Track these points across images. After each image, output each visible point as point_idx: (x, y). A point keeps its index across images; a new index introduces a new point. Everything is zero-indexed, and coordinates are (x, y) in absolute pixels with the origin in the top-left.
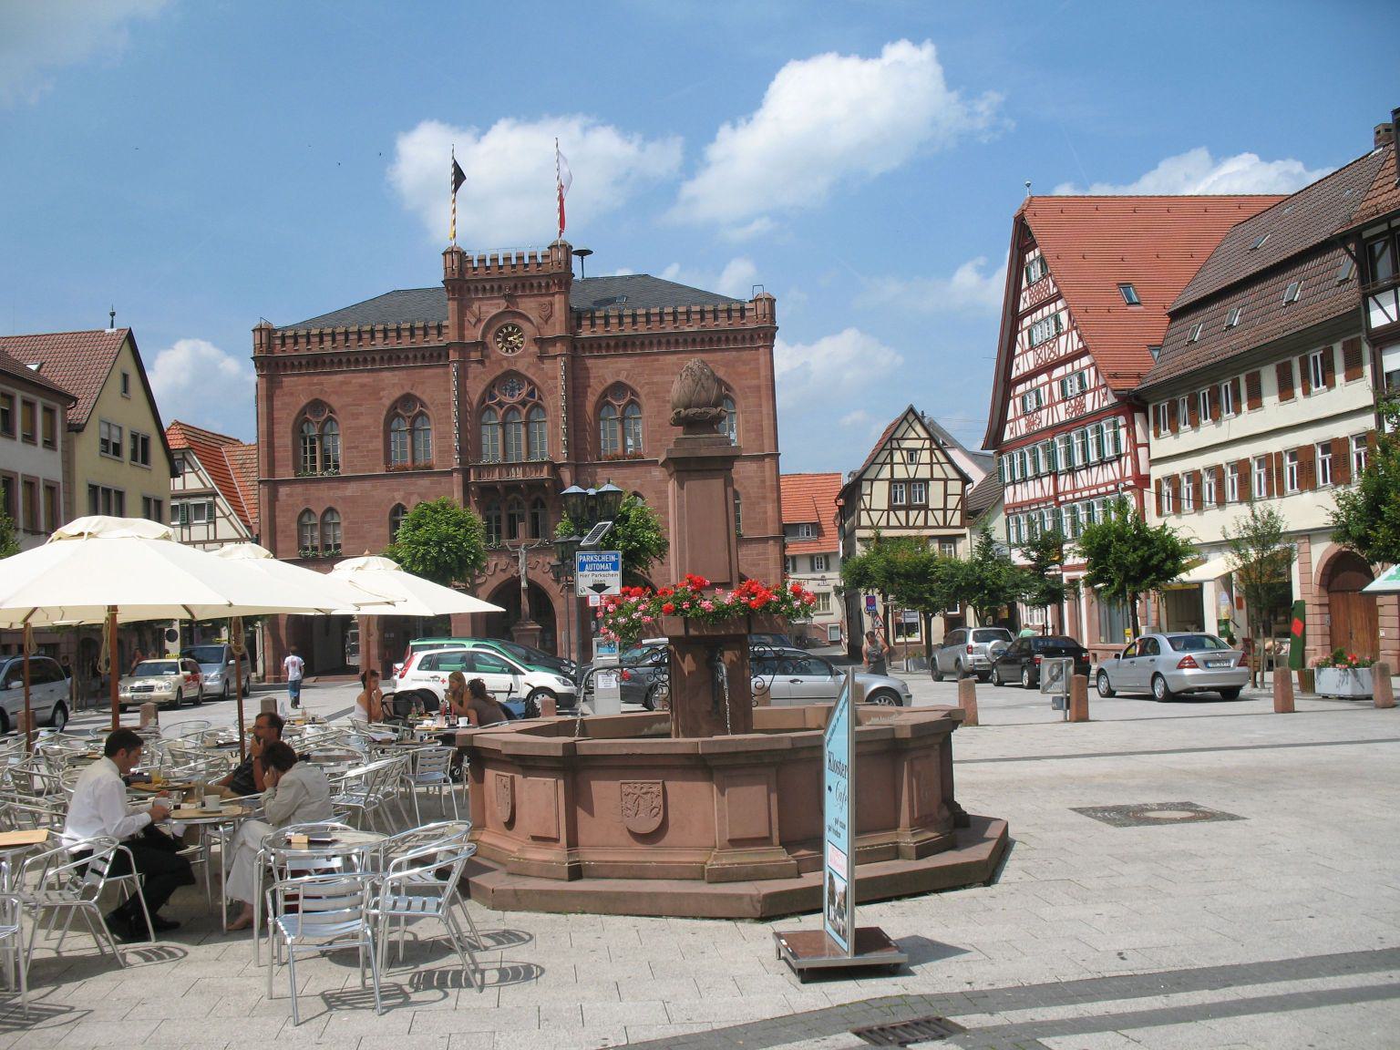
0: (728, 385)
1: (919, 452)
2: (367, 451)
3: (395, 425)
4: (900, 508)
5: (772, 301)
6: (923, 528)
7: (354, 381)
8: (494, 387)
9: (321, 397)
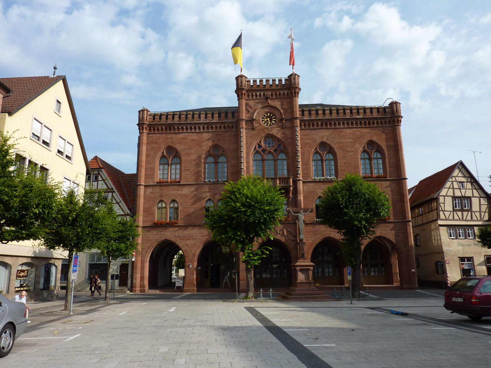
1: (465, 183)
4: (458, 210)
6: (469, 221)
7: (189, 137)
9: (171, 145)
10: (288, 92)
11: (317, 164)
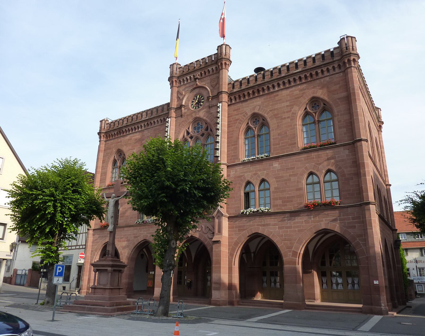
0: (325, 101)
7: (133, 138)
9: (120, 148)
10: (216, 67)
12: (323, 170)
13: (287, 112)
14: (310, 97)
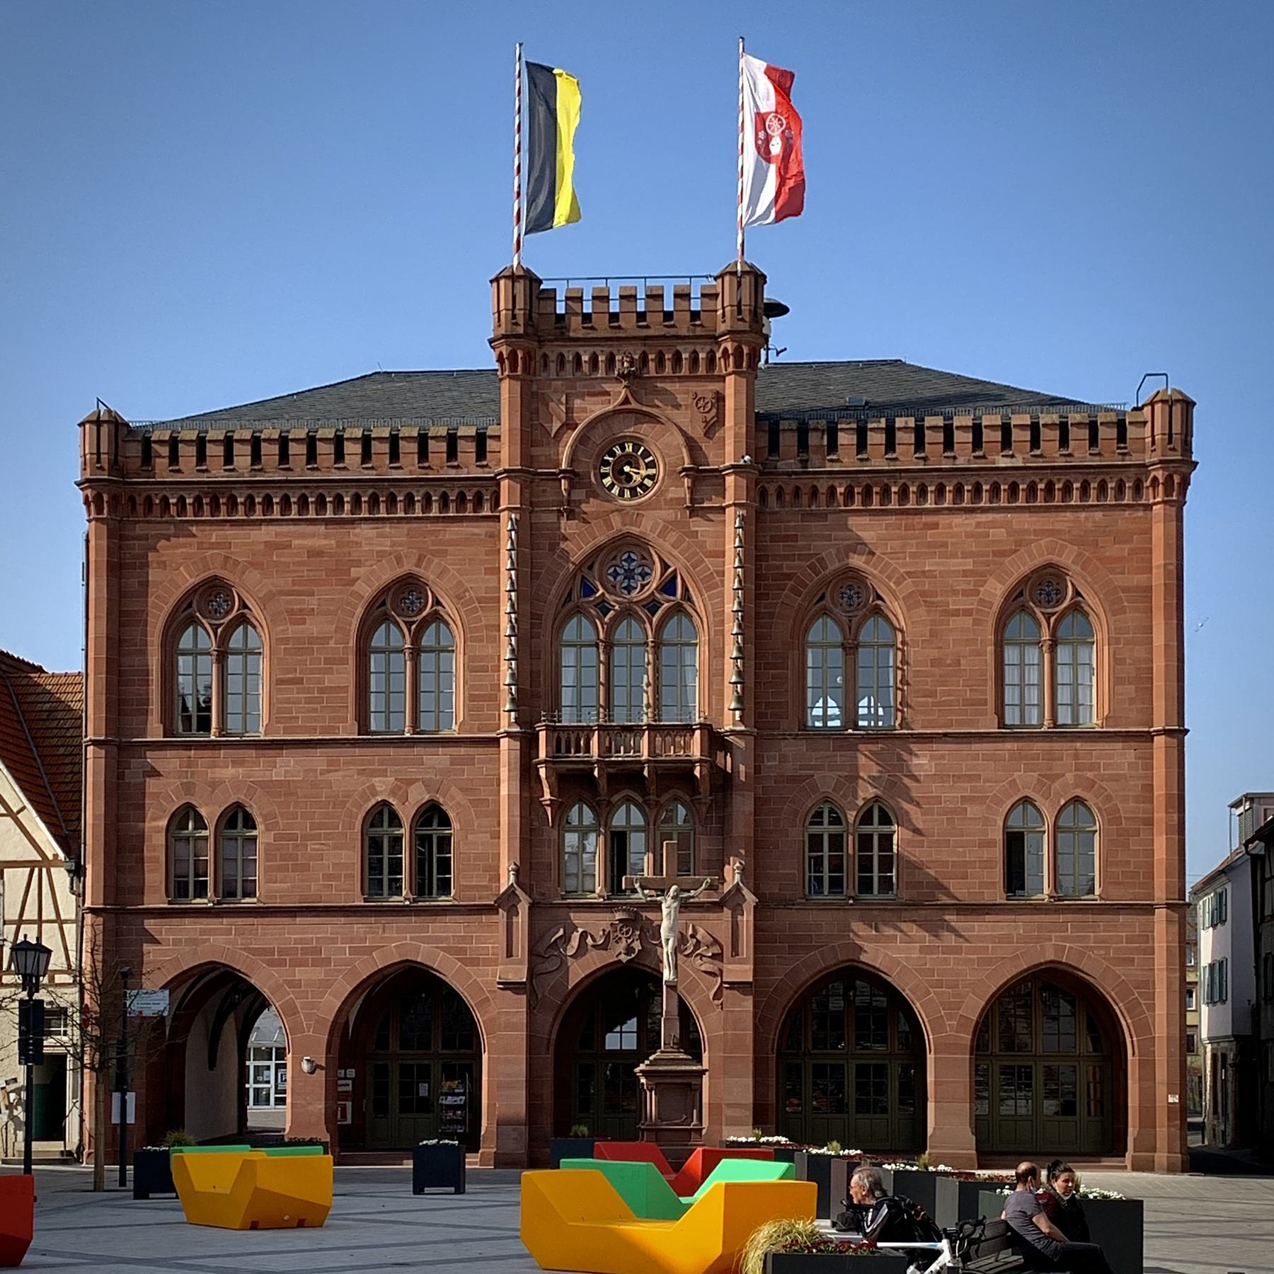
2: (321, 691)
3: (378, 640)
5: (1188, 405)
7: (295, 542)
8: (590, 568)
11: (824, 660)
12: (1061, 796)
13: (966, 593)
14: (1039, 561)
